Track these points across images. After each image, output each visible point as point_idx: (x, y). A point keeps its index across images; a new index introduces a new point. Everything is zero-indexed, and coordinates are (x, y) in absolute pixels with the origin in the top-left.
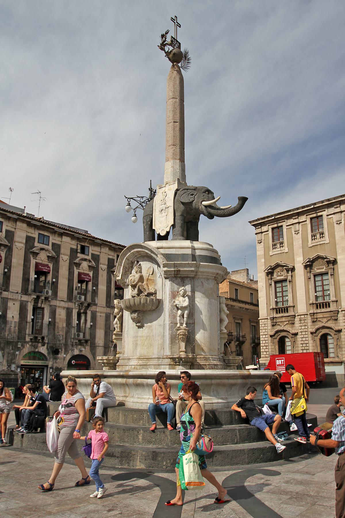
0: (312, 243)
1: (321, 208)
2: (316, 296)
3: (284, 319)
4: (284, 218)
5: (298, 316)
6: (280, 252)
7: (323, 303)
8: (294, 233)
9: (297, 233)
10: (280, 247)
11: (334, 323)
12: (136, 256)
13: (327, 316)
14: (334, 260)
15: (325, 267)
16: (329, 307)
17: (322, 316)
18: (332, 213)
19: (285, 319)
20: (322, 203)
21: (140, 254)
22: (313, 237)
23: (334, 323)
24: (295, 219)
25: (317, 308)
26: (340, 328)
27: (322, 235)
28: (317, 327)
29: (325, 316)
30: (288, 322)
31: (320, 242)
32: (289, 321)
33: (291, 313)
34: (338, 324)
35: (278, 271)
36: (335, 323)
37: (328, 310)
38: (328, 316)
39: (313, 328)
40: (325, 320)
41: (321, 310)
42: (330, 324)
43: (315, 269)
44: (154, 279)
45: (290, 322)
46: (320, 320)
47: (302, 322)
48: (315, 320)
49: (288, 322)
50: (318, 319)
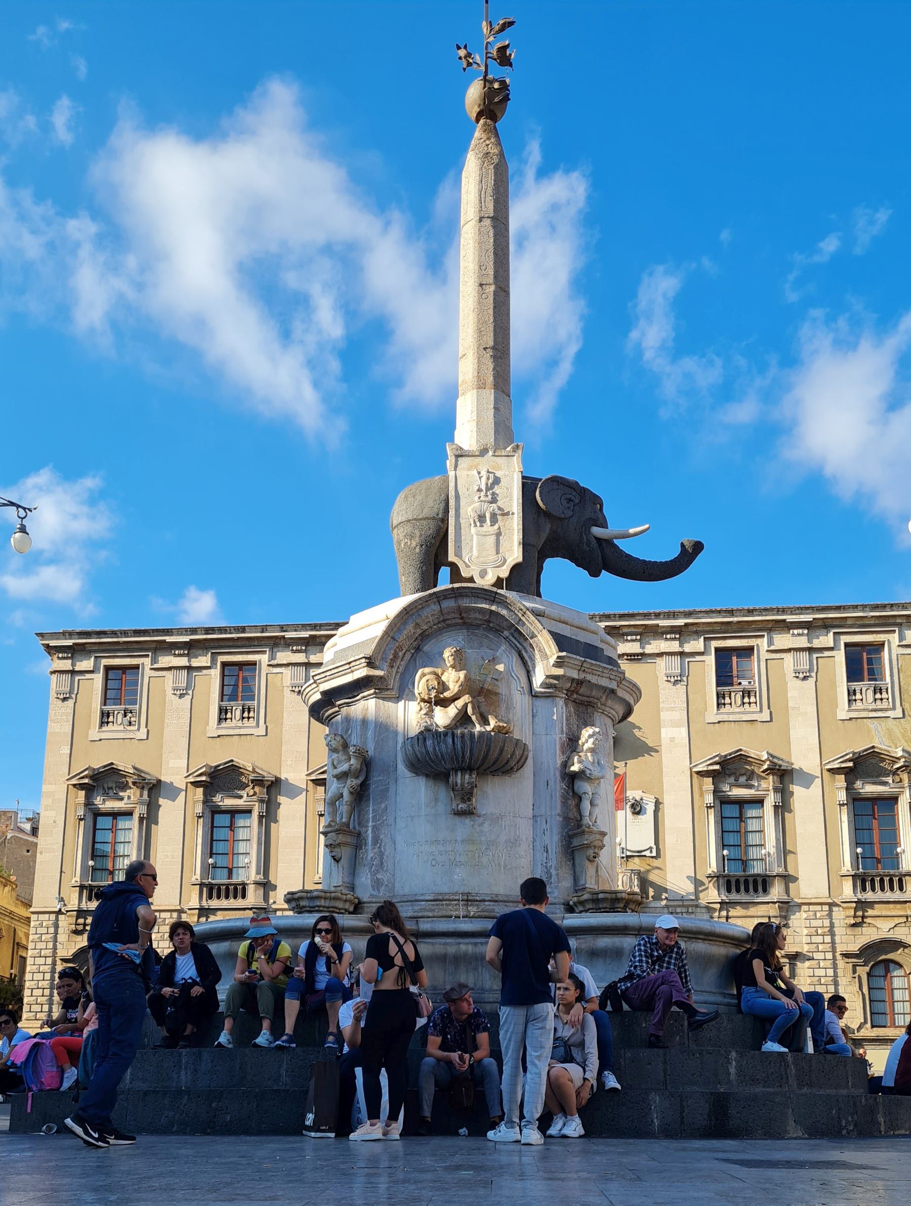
0: (217, 728)
1: (256, 643)
4: (146, 646)
6: (121, 735)
7: (227, 886)
8: (169, 691)
9: (178, 693)
10: (243, 718)
14: (272, 782)
15: (245, 795)
16: (244, 896)
18: (285, 662)
20: (262, 632)
21: (462, 618)
22: (223, 714)
24: (180, 655)
27: (249, 712)
31: (240, 728)
35: (110, 785)
37: (240, 903)
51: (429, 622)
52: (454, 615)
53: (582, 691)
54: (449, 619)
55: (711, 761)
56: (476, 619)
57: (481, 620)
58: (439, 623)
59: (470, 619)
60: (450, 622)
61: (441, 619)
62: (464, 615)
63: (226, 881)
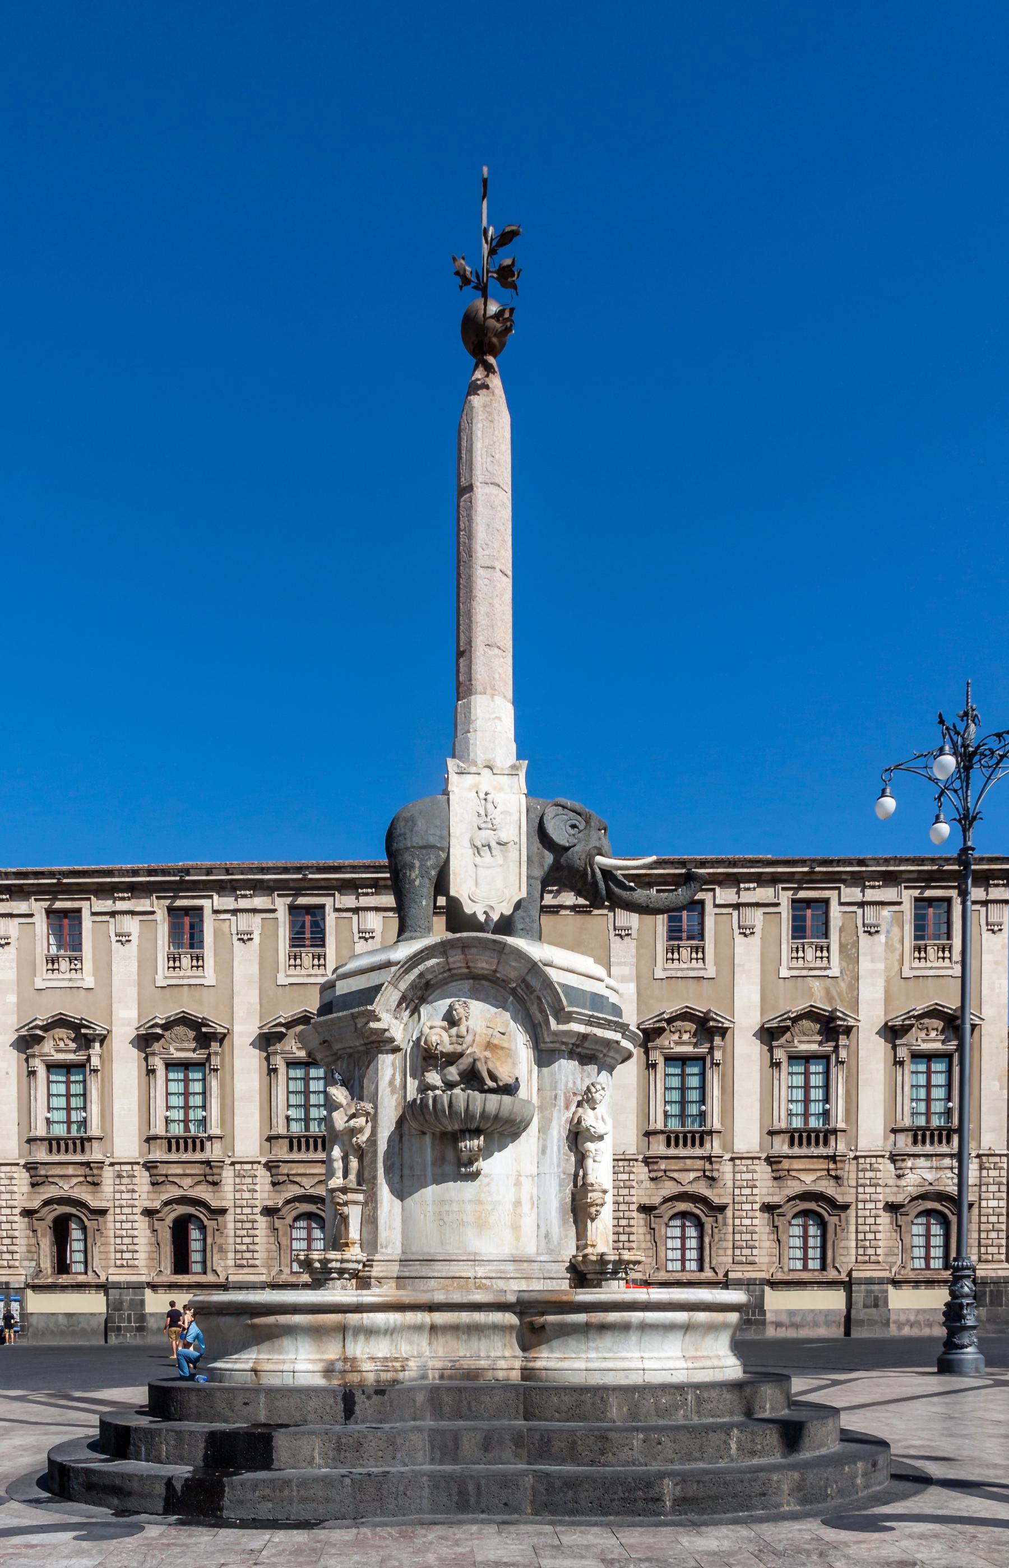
2: (166, 1118)
3: (70, 1170)
5: (112, 1164)
11: (210, 1190)
12: (450, 970)
13: (193, 1172)
16: (202, 1149)
17: (179, 1171)
19: (75, 1169)
21: (468, 967)
23: (210, 1190)
25: (170, 1150)
26: (225, 1204)
28: (164, 1197)
29: (188, 1172)
30: (81, 1179)
32: (86, 1176)
33: (95, 1154)
34: (222, 1194)
36: (214, 1192)
38: (198, 1172)
39: (153, 1200)
40: (187, 1182)
41: (179, 1155)
42: (202, 1192)
43: (172, 1050)
44: (513, 1047)
45: (89, 1179)
46: (175, 1180)
47: (125, 1181)
48: (161, 1180)
49: (81, 1179)
50: (171, 1179)
51: (435, 971)
52: (459, 965)
53: (585, 1045)
54: (454, 969)
55: (655, 1020)
56: (483, 968)
57: (488, 970)
58: (444, 972)
59: (475, 968)
60: (455, 971)
61: (447, 968)
62: (471, 964)
63: (182, 1133)
